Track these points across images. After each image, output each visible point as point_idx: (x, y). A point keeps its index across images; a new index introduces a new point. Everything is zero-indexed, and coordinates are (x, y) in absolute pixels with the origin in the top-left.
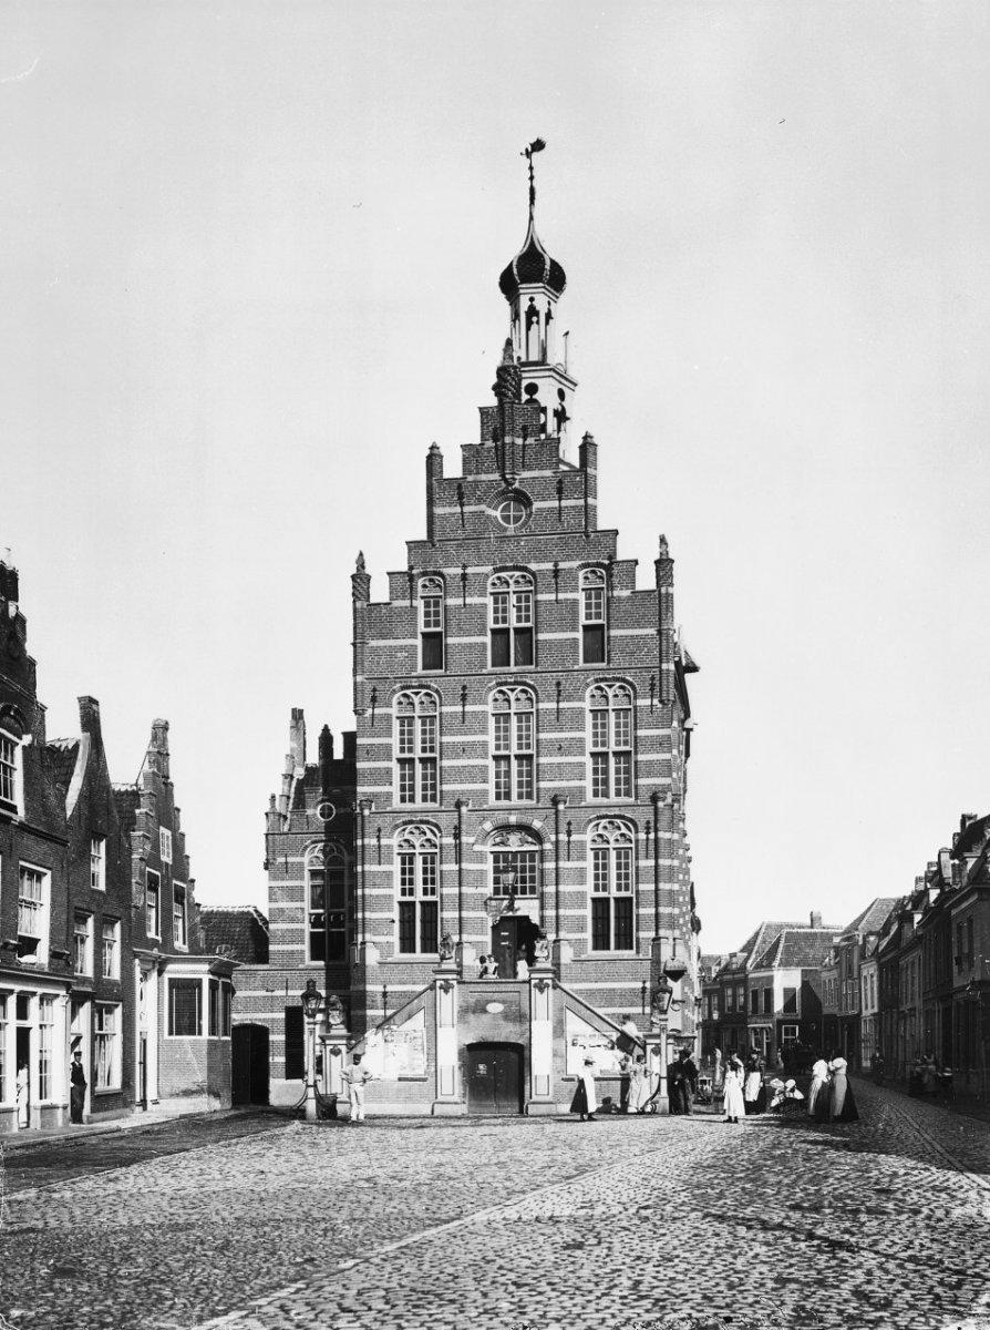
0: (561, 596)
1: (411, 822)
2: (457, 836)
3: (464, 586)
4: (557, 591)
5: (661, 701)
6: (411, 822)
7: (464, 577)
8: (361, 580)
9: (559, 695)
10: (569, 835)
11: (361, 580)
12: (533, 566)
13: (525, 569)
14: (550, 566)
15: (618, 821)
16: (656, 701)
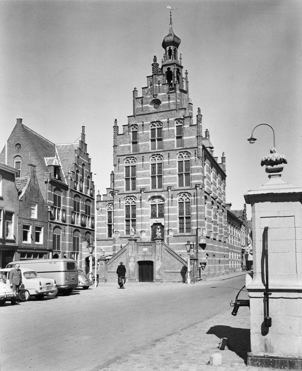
0: (170, 128)
1: (129, 196)
2: (141, 200)
3: (143, 128)
4: (168, 127)
5: (198, 157)
6: (129, 196)
7: (143, 125)
8: (116, 128)
9: (169, 157)
10: (172, 198)
11: (116, 128)
12: (162, 121)
13: (159, 122)
14: (166, 120)
15: (186, 194)
16: (196, 158)
